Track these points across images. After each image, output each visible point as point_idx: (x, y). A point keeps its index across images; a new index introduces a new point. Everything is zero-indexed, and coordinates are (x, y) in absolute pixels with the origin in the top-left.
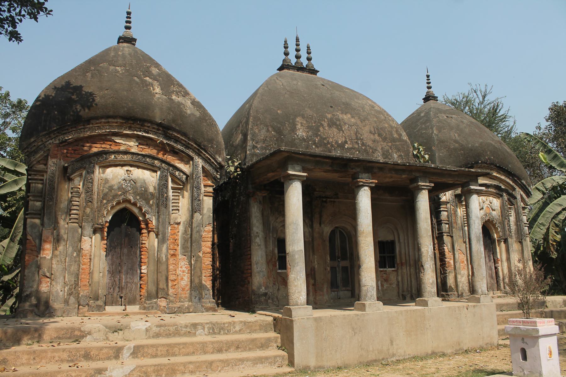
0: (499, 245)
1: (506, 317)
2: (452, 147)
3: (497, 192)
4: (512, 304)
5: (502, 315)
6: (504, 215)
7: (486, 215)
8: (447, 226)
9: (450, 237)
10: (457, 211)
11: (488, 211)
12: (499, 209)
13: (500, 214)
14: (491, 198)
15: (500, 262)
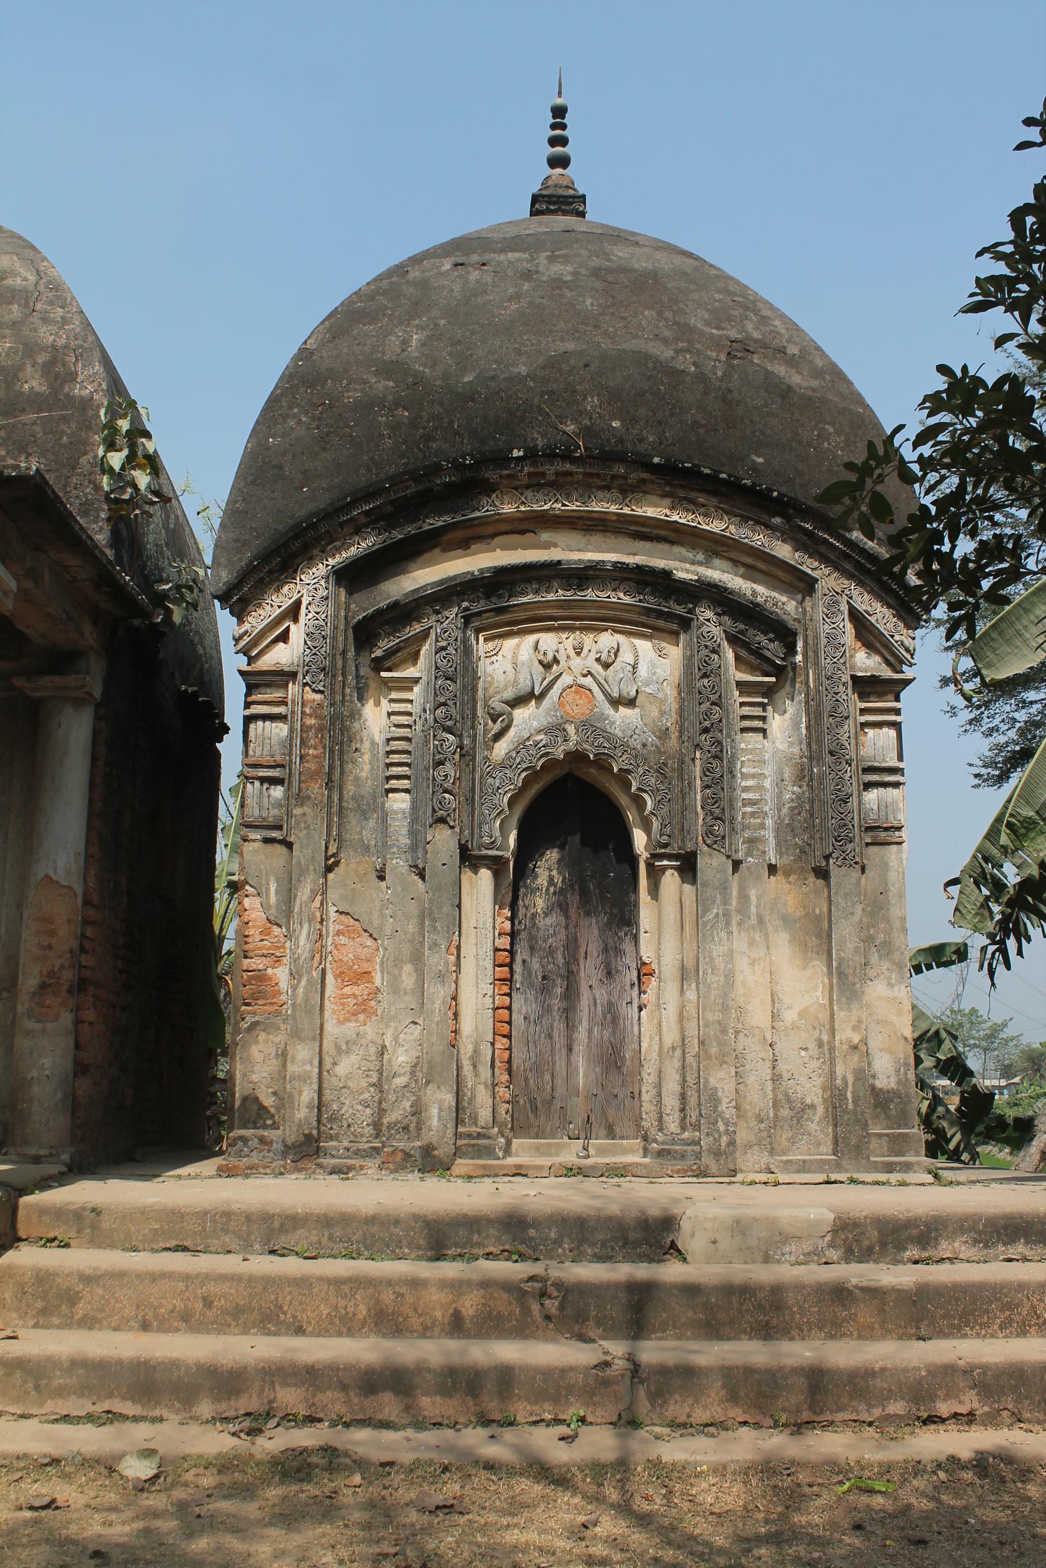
0: (654, 891)
1: (213, 1288)
2: (353, 395)
3: (651, 602)
4: (371, 1220)
5: (186, 1278)
6: (704, 727)
7: (556, 730)
8: (277, 792)
9: (281, 850)
10: (355, 715)
11: (578, 709)
12: (670, 693)
13: (670, 721)
14: (607, 640)
15: (654, 982)
